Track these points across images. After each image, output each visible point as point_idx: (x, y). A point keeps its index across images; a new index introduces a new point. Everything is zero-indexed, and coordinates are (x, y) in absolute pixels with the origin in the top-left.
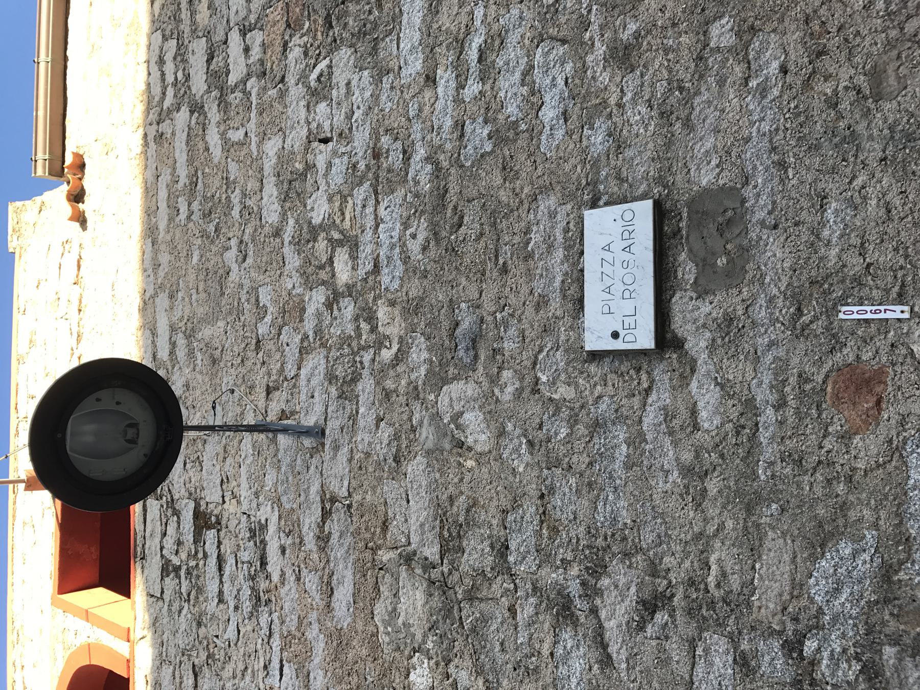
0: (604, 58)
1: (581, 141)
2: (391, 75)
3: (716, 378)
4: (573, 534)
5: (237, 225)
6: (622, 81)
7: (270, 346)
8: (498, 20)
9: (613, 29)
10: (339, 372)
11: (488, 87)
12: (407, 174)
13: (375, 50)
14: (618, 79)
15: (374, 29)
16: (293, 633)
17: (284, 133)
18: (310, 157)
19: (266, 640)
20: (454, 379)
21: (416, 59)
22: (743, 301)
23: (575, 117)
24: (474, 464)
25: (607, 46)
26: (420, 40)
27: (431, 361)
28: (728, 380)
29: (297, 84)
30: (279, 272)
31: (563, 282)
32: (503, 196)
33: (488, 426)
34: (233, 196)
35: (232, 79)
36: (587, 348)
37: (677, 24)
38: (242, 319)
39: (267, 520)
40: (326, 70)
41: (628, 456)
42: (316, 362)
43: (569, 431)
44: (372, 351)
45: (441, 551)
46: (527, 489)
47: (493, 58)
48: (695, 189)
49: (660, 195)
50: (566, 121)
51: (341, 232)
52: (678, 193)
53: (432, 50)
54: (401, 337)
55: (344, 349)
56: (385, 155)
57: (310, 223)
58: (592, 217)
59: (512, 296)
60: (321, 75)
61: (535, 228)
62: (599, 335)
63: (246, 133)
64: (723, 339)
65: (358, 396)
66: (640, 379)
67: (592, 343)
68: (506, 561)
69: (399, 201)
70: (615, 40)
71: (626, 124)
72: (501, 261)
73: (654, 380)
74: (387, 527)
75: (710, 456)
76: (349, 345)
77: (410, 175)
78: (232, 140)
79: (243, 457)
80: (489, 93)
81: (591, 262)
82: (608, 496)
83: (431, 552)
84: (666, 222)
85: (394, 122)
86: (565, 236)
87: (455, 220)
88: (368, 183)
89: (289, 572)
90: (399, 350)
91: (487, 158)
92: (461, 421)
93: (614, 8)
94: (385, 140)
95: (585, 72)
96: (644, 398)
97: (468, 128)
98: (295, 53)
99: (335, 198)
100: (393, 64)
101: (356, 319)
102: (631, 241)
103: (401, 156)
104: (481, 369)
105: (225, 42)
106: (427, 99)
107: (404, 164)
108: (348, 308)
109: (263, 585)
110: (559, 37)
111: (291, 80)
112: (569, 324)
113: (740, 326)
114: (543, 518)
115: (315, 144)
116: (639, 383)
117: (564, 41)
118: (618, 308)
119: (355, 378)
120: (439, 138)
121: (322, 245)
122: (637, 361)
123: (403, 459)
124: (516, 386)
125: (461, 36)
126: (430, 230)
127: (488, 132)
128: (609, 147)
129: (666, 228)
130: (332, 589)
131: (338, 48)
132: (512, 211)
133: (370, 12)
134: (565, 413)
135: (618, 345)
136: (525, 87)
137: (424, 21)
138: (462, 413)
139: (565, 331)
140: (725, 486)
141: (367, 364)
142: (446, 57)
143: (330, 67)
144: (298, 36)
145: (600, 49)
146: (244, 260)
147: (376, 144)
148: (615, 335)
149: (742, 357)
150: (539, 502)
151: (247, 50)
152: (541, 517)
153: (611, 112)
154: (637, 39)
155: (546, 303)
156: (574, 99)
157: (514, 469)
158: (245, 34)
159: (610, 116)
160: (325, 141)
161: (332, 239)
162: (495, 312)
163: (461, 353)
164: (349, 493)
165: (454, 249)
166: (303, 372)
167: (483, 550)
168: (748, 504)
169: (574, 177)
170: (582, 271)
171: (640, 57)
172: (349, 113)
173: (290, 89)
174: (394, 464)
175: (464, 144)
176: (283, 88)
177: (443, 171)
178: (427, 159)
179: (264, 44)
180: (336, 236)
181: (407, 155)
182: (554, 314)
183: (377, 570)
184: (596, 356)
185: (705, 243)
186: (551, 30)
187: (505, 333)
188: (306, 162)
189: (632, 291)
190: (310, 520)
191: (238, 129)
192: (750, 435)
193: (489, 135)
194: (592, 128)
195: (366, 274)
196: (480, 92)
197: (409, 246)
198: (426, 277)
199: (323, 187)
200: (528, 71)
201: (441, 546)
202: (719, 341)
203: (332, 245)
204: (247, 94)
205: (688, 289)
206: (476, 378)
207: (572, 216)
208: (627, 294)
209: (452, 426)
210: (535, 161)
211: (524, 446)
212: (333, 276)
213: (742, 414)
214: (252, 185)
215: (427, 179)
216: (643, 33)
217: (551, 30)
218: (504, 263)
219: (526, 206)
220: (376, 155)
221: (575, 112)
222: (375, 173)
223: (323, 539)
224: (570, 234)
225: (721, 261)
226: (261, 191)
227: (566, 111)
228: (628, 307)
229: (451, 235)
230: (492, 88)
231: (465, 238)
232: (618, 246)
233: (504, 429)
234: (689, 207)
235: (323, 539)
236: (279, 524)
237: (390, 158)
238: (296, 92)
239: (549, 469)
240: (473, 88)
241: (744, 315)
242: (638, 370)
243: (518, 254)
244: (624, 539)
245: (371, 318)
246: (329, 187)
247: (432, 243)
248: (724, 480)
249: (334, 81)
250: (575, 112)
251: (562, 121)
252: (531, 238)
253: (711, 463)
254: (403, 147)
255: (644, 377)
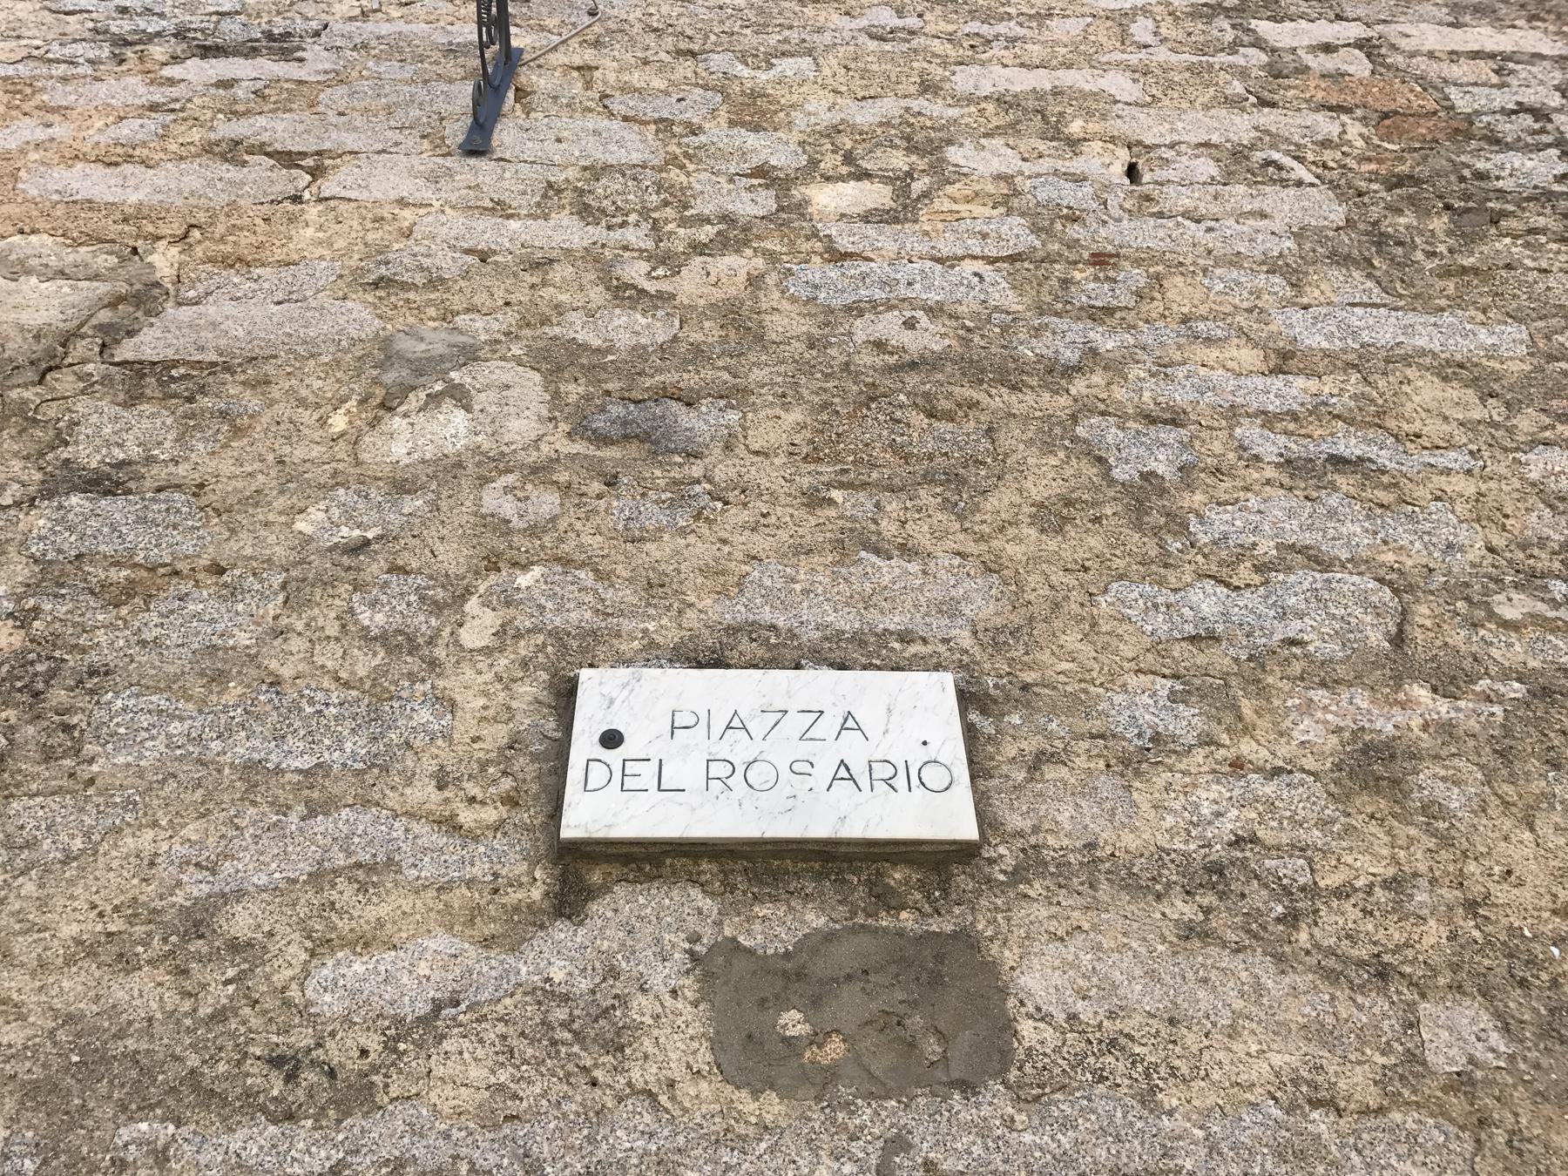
0: (1363, 729)
1: (1139, 671)
2: (1289, 292)
3: (458, 1004)
4: (101, 637)
5: (951, 28)
6: (1303, 771)
7: (685, 68)
8: (1438, 499)
9: (1444, 753)
10: (610, 185)
11: (1270, 472)
12: (1057, 314)
13: (1340, 259)
14: (1309, 763)
15: (1392, 260)
16: (38, 96)
17: (1148, 105)
18: (1097, 145)
19: (35, 53)
20: (556, 395)
21: (1329, 337)
22: (671, 1084)
23: (1201, 659)
24: (337, 430)
25: (1394, 738)
26: (1373, 345)
27: (609, 351)
28: (444, 1037)
29: (1256, 128)
30: (843, 89)
31: (773, 627)
32: (1000, 501)
33: (424, 461)
34: (1012, 24)
35: (1264, 27)
36: (585, 674)
37: (1476, 915)
38: (748, 31)
39: (301, 60)
40: (1293, 176)
41: (278, 771)
42: (634, 147)
43: (375, 632)
44: (649, 244)
45: (141, 363)
46: (243, 535)
47: (1344, 488)
48: (1007, 953)
49: (991, 861)
50: (1192, 639)
51: (925, 195)
52: (997, 909)
53: (1355, 366)
54: (673, 296)
55: (658, 193)
56: (1101, 275)
57: (950, 142)
58: (939, 690)
59: (745, 516)
60: (1280, 168)
61: (914, 567)
62: (618, 702)
63: (1146, 47)
64: (565, 1025)
65: (546, 217)
66: (483, 803)
67: (594, 685)
68: (75, 489)
69: (996, 299)
70: (1413, 756)
71: (1187, 779)
72: (836, 495)
73: (476, 839)
74: (232, 266)
75: (227, 982)
76: (666, 203)
77: (1055, 319)
78: (1133, 26)
79: (449, 28)
80: (1256, 475)
81: (818, 684)
82: (181, 719)
83: (148, 344)
84: (915, 877)
85: (1180, 293)
86: (892, 633)
87: (942, 402)
88: (1037, 243)
89: (174, 92)
90: (643, 291)
91: (1095, 470)
92: (448, 404)
93: (1501, 754)
94: (1137, 277)
95: (1323, 684)
96: (431, 813)
97: (1170, 435)
98: (1327, 126)
99: (1002, 184)
100: (1311, 295)
101: (726, 218)
102: (864, 782)
103: (1099, 304)
104: (579, 447)
105: (1339, 17)
106: (1235, 353)
107: (1081, 308)
108: (753, 204)
109: (158, 51)
110: (1407, 627)
111: (1268, 118)
112: (660, 640)
113: (598, 1074)
114: (162, 571)
115: (1124, 156)
116: (472, 800)
117: (1399, 639)
118: (687, 746)
119: (586, 212)
120: (1142, 375)
121: (899, 161)
122: (536, 797)
123: (382, 293)
124: (515, 519)
125: (1391, 423)
126: (922, 356)
127: (1160, 472)
128: (1125, 739)
129: (897, 876)
130: (117, 164)
131: (1341, 198)
132: (961, 517)
133: (1431, 255)
134: (422, 622)
135: (584, 744)
136: (1274, 552)
137: (1423, 352)
138: (468, 408)
139: (645, 631)
140: (130, 1023)
141: (617, 234)
142: (1338, 389)
143: (1299, 183)
144: (1364, 130)
145: (1385, 725)
146: (872, 37)
147: (1127, 258)
148: (611, 739)
149: (503, 1076)
150: (204, 561)
151: (1328, 48)
152: (166, 565)
153: (1219, 745)
154: (1424, 809)
155: (723, 593)
156: (1249, 659)
157: (301, 511)
158: (1360, 47)
159: (1208, 741)
160: (1132, 172)
161: (913, 179)
162: (710, 481)
163: (616, 410)
164: (327, 199)
165: (873, 399)
166: (616, 125)
167: (120, 446)
168: (55, 1088)
169: (1045, 657)
170: (798, 667)
171: (1372, 817)
172: (1196, 215)
173: (1246, 116)
174: (372, 278)
175: (1130, 424)
176: (1247, 104)
177: (1063, 382)
178: (1094, 352)
179: (1342, 75)
180: (917, 187)
181: (1100, 314)
182: (691, 605)
183: (131, 243)
184: (565, 696)
185: (849, 977)
186: (1424, 610)
187: (656, 502)
188: (1085, 140)
189: (729, 782)
190: (280, 130)
191: (1156, 34)
192: (261, 1098)
193: (1153, 473)
194: (1173, 697)
195: (828, 236)
196: (1257, 458)
197: (889, 315)
198: (811, 346)
199: (1027, 168)
200: (1318, 561)
201: (154, 363)
202: (561, 1014)
203: (898, 178)
204: (1233, 48)
205: (721, 931)
206: (552, 439)
207: (942, 648)
208: (719, 770)
209: (438, 387)
210: (1086, 569)
211: (357, 533)
212: (828, 179)
213: (332, 1074)
214: (1035, 51)
215: (1045, 352)
216: (1442, 825)
217: (1424, 610)
218: (831, 502)
219: (971, 547)
220: (1100, 260)
221: (1219, 658)
222: (1061, 255)
223: (232, 153)
224: (897, 645)
225: (793, 1023)
226: (1022, 65)
227: (1217, 639)
228: (685, 770)
229: (908, 394)
230: (1268, 482)
231: (899, 422)
232: (855, 750)
233: (408, 492)
234: (954, 935)
235: (232, 153)
236: (287, 81)
237: (1092, 285)
238: (1240, 127)
239: (284, 586)
240: (1270, 446)
241: (629, 1084)
242: (511, 801)
243: (852, 530)
244: (48, 756)
245: (723, 244)
246: (1030, 177)
247: (892, 360)
248: (150, 1020)
249: (1268, 189)
250: (1219, 658)
251: (1190, 629)
252: (890, 558)
253: (204, 986)
254: (1120, 309)
255: (490, 814)
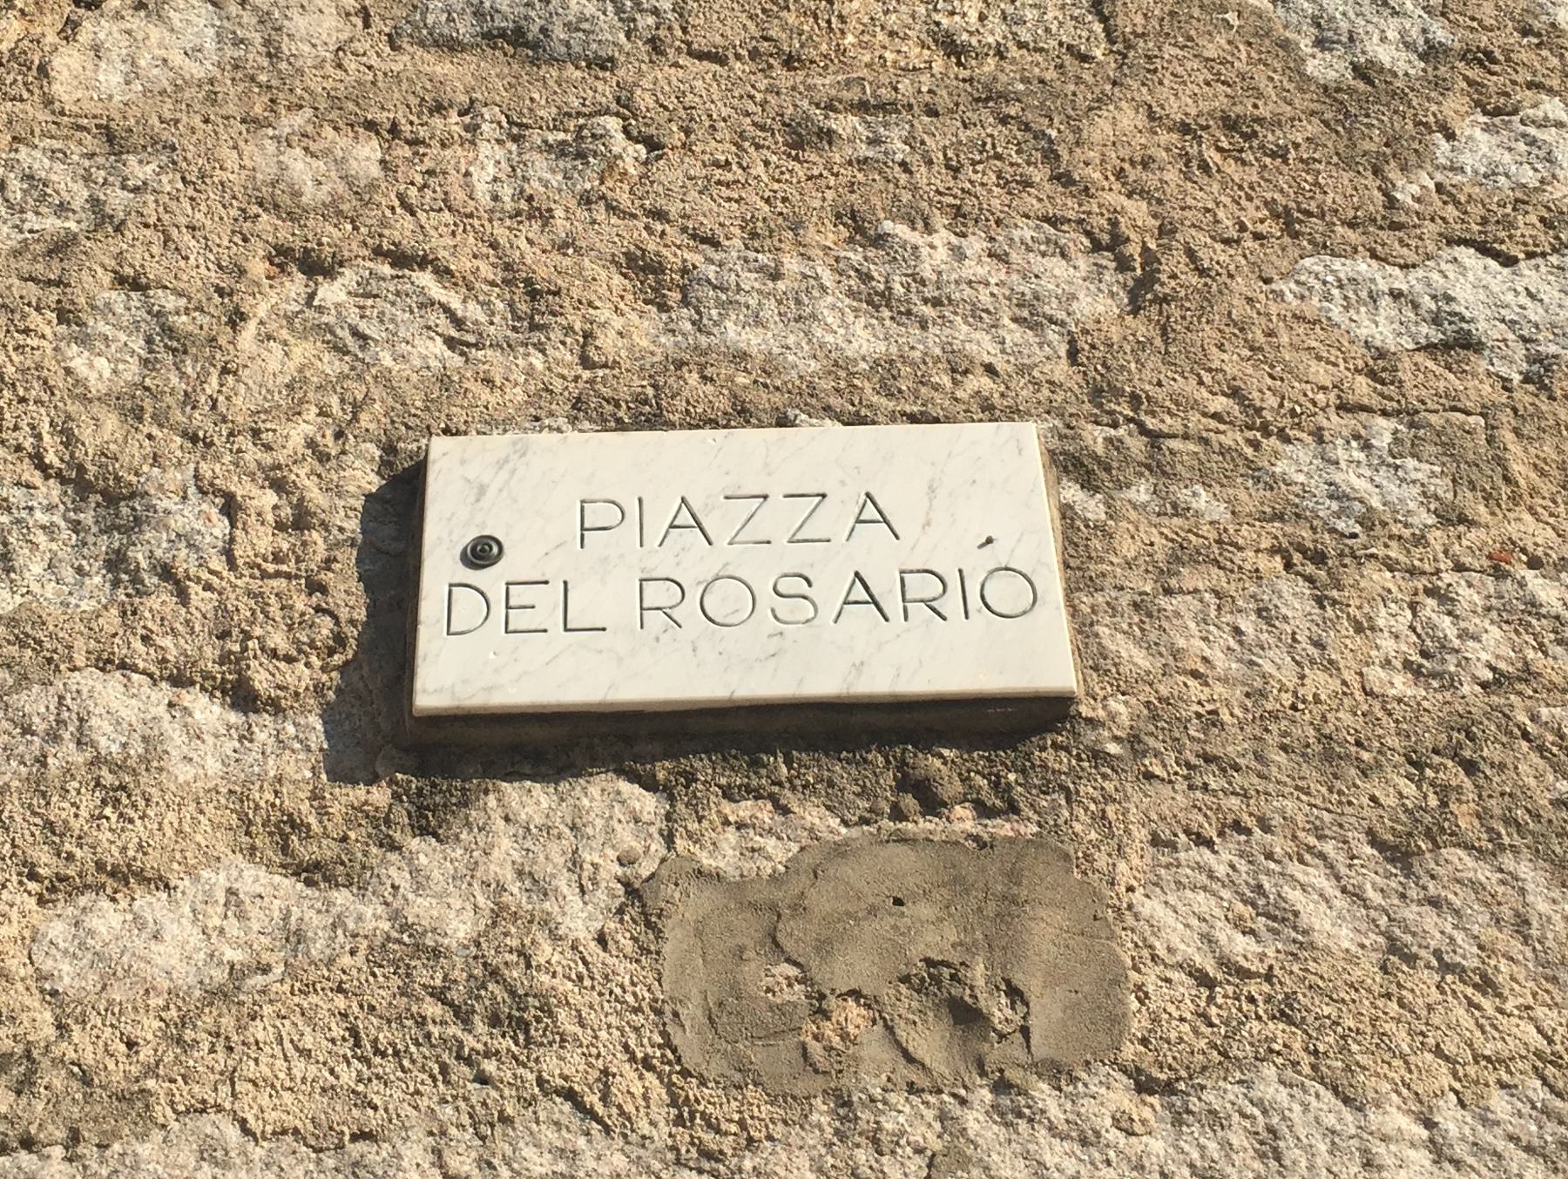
36: (440, 447)
48: (1122, 866)
52: (1109, 799)
62: (492, 492)
102: (893, 605)
113: (490, 1066)
148: (481, 553)
153: (1471, 523)
170: (783, 422)
185: (872, 911)
189: (675, 614)
208: (658, 594)
218: (829, 136)
234: (1037, 842)
251: (1427, 332)
